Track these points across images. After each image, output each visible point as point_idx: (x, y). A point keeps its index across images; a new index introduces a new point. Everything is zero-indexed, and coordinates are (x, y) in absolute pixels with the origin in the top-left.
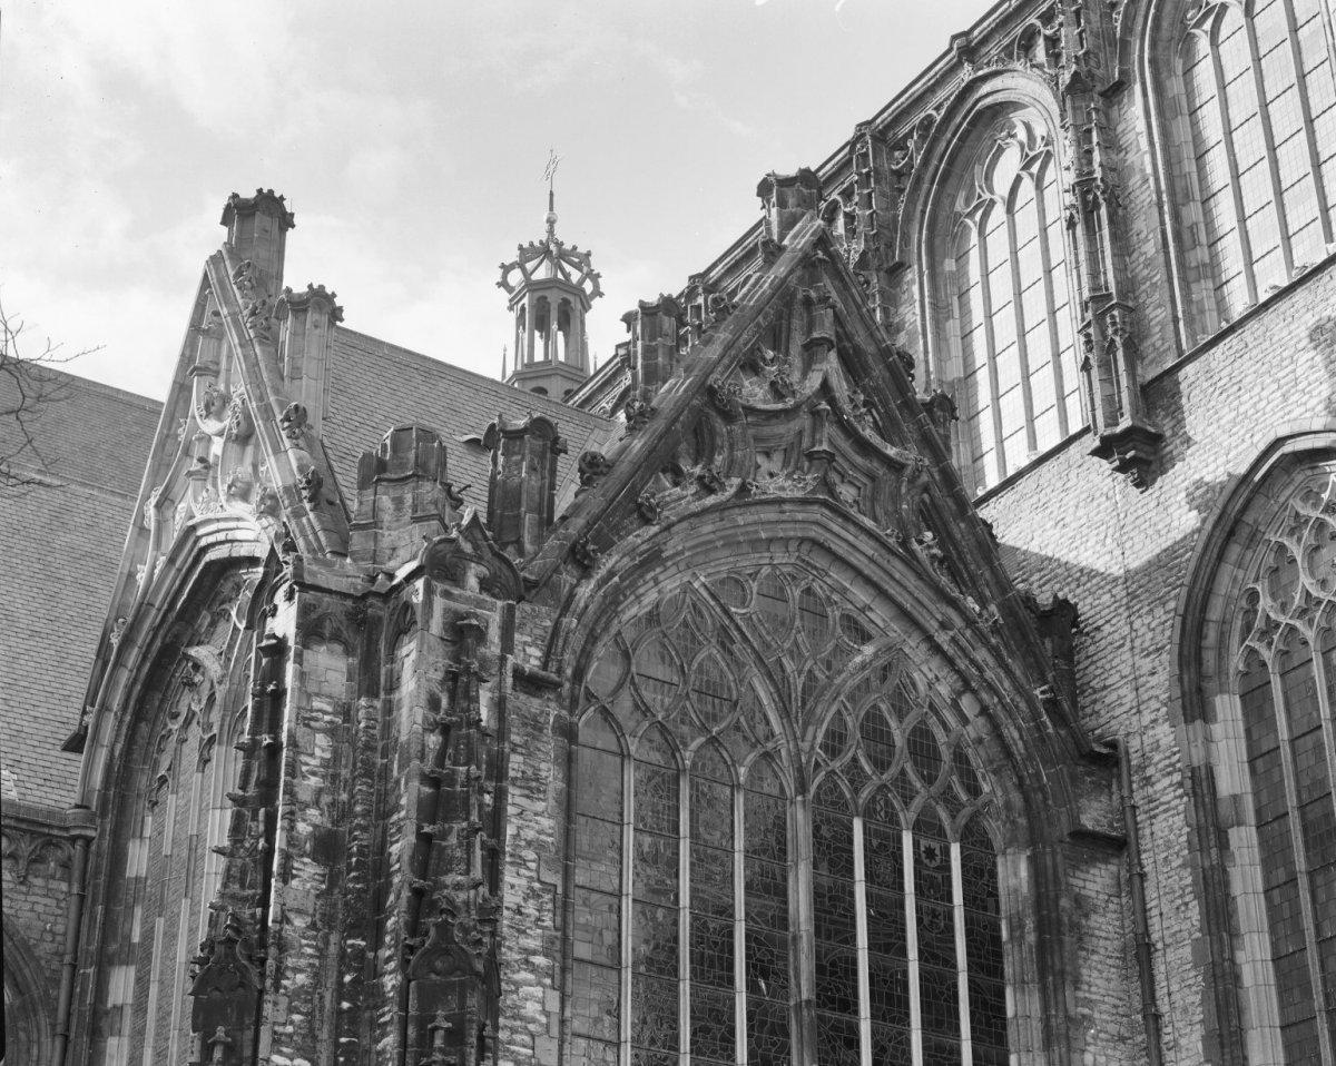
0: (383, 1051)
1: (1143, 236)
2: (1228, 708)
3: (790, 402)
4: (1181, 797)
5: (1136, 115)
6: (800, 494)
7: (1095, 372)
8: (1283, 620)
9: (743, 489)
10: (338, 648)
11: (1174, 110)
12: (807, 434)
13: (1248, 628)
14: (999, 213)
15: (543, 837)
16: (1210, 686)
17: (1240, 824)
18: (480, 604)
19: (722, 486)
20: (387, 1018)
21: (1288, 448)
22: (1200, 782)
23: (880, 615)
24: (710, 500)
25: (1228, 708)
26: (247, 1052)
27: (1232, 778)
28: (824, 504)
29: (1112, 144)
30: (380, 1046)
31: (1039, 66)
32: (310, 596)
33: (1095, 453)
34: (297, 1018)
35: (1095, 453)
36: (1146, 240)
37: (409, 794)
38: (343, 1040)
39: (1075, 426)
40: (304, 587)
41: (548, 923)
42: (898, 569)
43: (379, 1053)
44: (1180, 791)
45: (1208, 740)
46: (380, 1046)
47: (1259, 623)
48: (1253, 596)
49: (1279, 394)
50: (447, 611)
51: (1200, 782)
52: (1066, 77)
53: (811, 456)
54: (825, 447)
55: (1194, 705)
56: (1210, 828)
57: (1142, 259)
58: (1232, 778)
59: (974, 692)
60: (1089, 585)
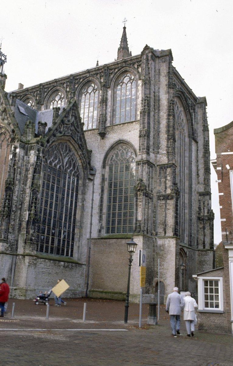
2: (107, 168)
3: (70, 123)
5: (110, 92)
8: (116, 160)
10: (23, 149)
11: (114, 93)
12: (70, 127)
13: (111, 160)
14: (88, 94)
16: (106, 165)
17: (107, 181)
18: (41, 148)
22: (103, 176)
23: (73, 149)
25: (107, 168)
26: (11, 197)
27: (107, 176)
28: (71, 136)
29: (107, 95)
31: (98, 79)
32: (21, 143)
37: (31, 171)
39: (94, 127)
40: (21, 141)
45: (105, 171)
47: (113, 159)
48: (113, 156)
50: (38, 148)
51: (103, 176)
52: (103, 84)
55: (104, 167)
56: (103, 180)
58: (107, 176)
59: (81, 160)
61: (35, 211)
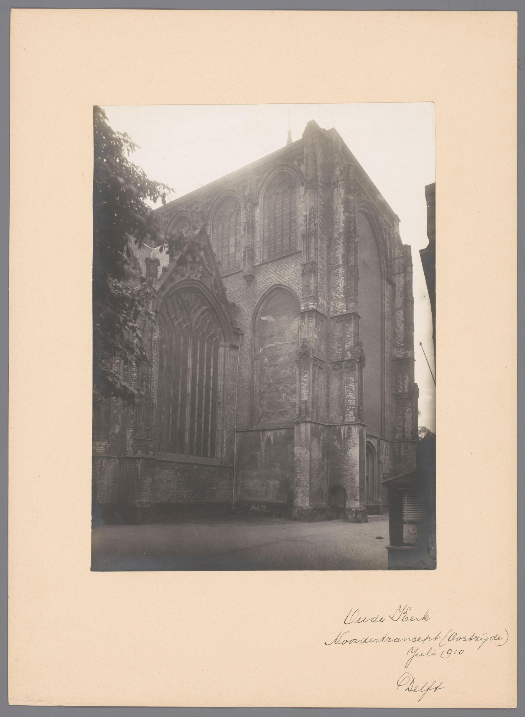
0: (134, 376)
1: (257, 236)
4: (249, 342)
6: (197, 279)
7: (247, 263)
9: (189, 277)
15: (155, 340)
19: (185, 276)
20: (134, 370)
21: (277, 286)
24: (183, 279)
30: (132, 375)
33: (243, 277)
34: (117, 368)
35: (243, 277)
36: (257, 238)
38: (125, 373)
41: (156, 355)
42: (210, 295)
43: (132, 376)
44: (249, 341)
46: (132, 375)
49: (277, 276)
53: (199, 271)
54: (201, 270)
57: (256, 241)
60: (237, 300)
61: (147, 392)
